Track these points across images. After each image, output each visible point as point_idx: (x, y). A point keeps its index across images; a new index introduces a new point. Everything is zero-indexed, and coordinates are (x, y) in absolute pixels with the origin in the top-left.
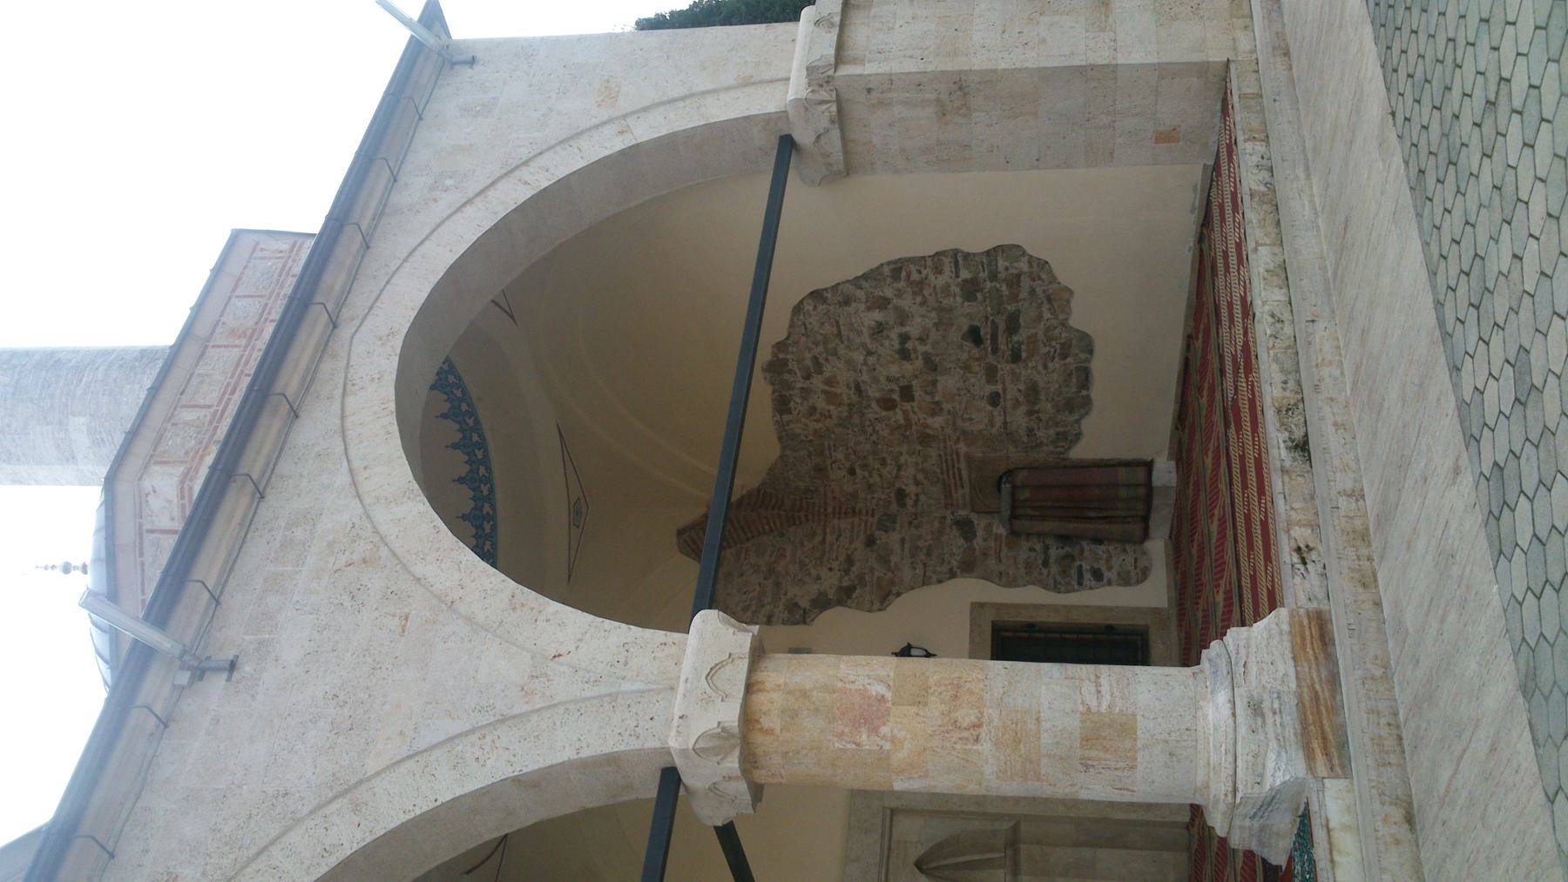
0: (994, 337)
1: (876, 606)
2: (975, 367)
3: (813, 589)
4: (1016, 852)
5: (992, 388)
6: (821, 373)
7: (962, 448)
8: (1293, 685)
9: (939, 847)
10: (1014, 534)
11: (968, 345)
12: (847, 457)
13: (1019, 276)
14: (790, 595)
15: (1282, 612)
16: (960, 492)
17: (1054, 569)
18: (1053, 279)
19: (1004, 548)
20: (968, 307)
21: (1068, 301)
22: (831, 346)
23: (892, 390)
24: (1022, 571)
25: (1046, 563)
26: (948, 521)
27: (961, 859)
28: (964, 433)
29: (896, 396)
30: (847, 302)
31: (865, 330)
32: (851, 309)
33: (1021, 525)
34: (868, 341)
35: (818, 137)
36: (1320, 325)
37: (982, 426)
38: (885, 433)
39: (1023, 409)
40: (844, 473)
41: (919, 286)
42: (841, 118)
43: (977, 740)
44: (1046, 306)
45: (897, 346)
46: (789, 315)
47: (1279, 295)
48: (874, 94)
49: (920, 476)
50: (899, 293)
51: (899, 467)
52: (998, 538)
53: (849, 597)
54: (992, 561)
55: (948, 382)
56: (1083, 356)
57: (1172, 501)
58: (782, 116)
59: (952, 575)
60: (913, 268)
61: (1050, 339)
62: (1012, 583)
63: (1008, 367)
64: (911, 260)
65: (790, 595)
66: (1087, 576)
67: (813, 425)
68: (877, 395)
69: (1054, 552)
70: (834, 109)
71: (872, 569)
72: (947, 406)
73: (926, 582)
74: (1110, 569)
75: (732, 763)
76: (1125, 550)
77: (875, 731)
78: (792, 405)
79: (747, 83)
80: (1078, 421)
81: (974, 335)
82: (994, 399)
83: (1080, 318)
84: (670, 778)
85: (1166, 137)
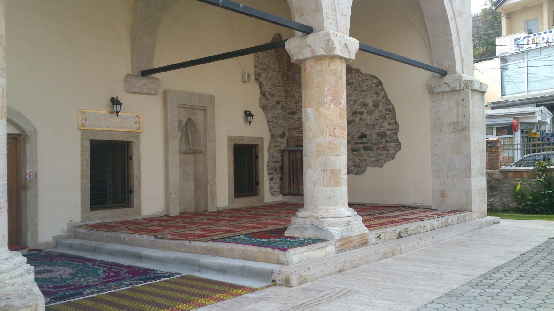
3: (264, 82)
4: (191, 153)
8: (354, 235)
10: (283, 152)
11: (359, 134)
15: (366, 231)
17: (273, 165)
18: (386, 161)
21: (377, 166)
22: (358, 88)
25: (274, 162)
30: (377, 93)
31: (365, 100)
32: (374, 95)
33: (286, 154)
34: (360, 101)
35: (447, 84)
36: (432, 240)
42: (454, 91)
43: (331, 135)
44: (375, 159)
45: (358, 111)
46: (371, 74)
47: (429, 229)
48: (462, 102)
50: (380, 111)
52: (281, 146)
56: (355, 172)
57: (299, 202)
58: (454, 71)
59: (270, 131)
60: (391, 115)
61: (361, 161)
62: (269, 151)
66: (271, 176)
70: (458, 89)
74: (273, 183)
75: (322, 52)
77: (332, 102)
79: (462, 60)
81: (363, 136)
84: (308, 31)
85: (443, 194)
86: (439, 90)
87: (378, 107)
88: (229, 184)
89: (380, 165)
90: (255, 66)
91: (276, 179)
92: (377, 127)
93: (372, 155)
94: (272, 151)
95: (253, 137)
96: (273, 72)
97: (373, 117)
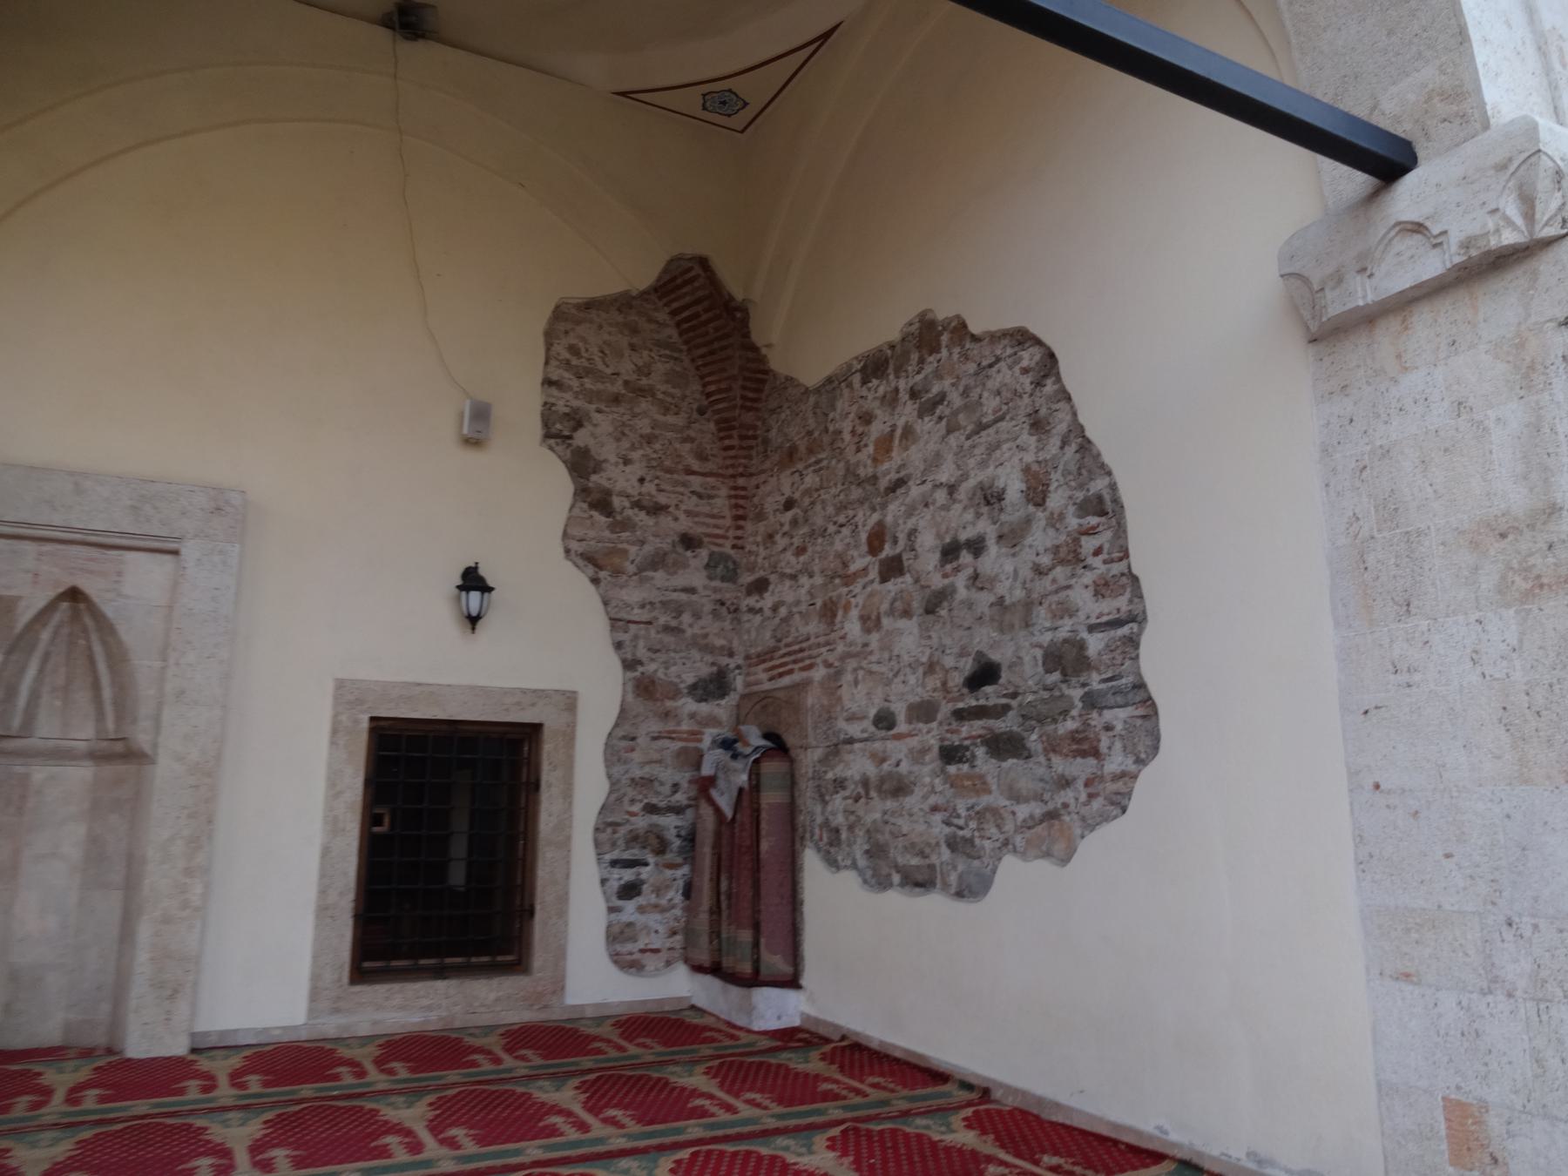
0: (981, 712)
1: (574, 546)
2: (934, 682)
3: (608, 451)
5: (901, 717)
6: (921, 416)
7: (819, 673)
9: (105, 627)
11: (968, 666)
12: (807, 492)
13: (1096, 753)
14: (597, 417)
16: (764, 676)
17: (641, 823)
18: (1089, 825)
19: (680, 744)
20: (1032, 662)
21: (1047, 855)
23: (895, 541)
24: (637, 773)
25: (651, 809)
26: (724, 661)
27: (102, 667)
28: (839, 673)
29: (888, 551)
30: (1038, 425)
31: (990, 470)
34: (972, 483)
35: (1418, 228)
37: (847, 704)
38: (839, 546)
39: (871, 770)
40: (787, 491)
41: (1071, 557)
44: (1037, 809)
45: (963, 536)
49: (783, 611)
50: (1055, 521)
51: (794, 577)
52: (695, 735)
53: (593, 506)
54: (655, 726)
55: (908, 638)
56: (953, 878)
59: (629, 665)
60: (1104, 538)
61: (980, 816)
63: (934, 743)
64: (1120, 531)
65: (597, 417)
66: (628, 875)
67: (846, 426)
68: (889, 519)
69: (670, 823)
70: (1509, 238)
71: (642, 543)
72: (874, 639)
73: (615, 623)
74: (641, 910)
76: (674, 933)
78: (875, 382)
80: (854, 866)
81: (985, 674)
82: (885, 721)
83: (1018, 877)
86: (1364, 293)
87: (1040, 504)
88: (323, 910)
89: (1058, 848)
90: (548, 382)
91: (658, 891)
92: (1042, 616)
93: (1025, 784)
94: (637, 756)
95: (507, 692)
96: (666, 410)
97: (1027, 557)
